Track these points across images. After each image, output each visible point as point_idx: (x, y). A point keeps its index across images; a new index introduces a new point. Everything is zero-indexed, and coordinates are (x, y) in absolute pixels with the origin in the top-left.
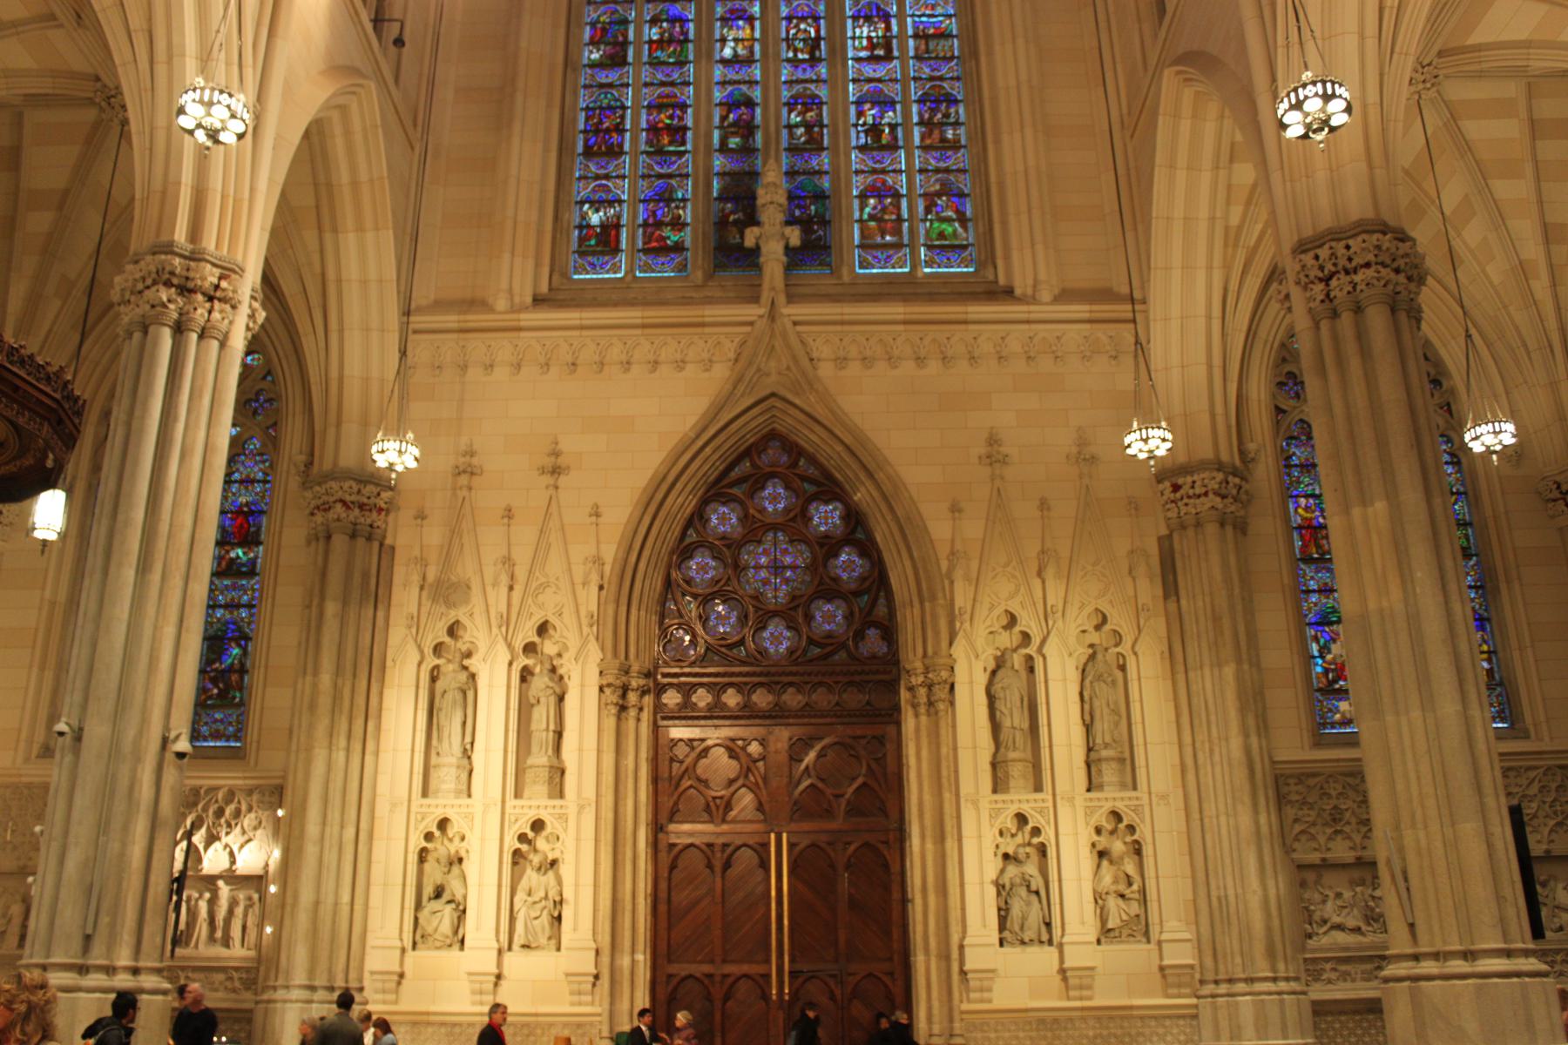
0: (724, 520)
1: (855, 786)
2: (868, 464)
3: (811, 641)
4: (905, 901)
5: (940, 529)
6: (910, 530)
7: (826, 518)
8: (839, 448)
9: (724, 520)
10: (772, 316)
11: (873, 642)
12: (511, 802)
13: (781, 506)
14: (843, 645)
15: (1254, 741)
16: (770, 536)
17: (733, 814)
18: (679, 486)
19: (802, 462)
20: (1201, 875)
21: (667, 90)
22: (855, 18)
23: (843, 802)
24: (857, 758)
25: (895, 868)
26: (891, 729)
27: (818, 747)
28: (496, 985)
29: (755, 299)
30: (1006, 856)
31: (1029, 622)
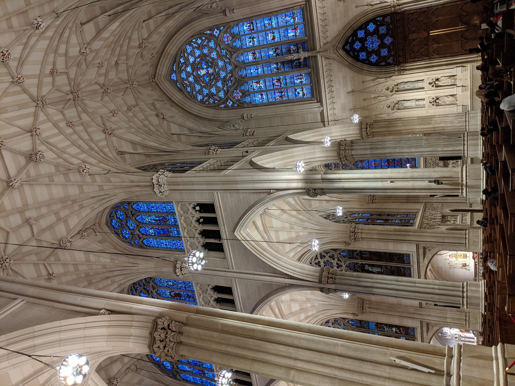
0: (363, 55)
7: (361, 34)
9: (363, 55)
10: (319, 52)
12: (425, 89)
28: (464, 86)
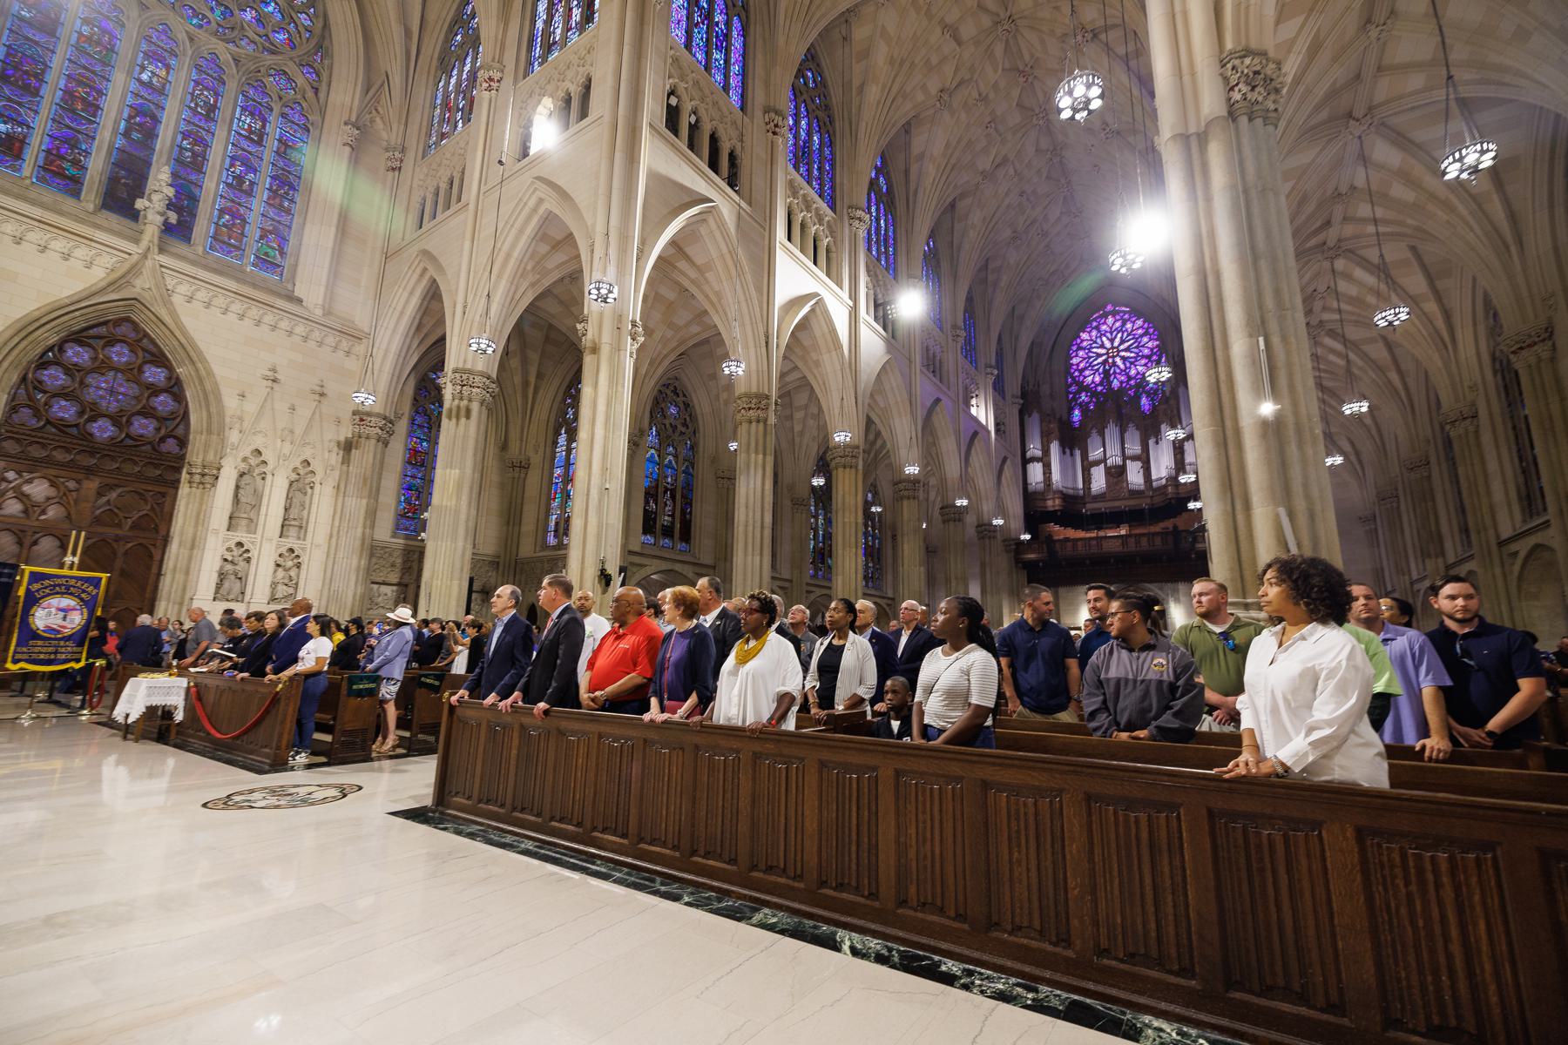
1: (141, 514)
2: (192, 355)
3: (128, 436)
4: (159, 574)
5: (230, 402)
6: (211, 397)
7: (154, 375)
8: (176, 343)
11: (170, 446)
13: (124, 359)
14: (150, 443)
15: (368, 530)
16: (112, 373)
17: (43, 517)
18: (48, 327)
19: (145, 341)
20: (327, 581)
21: (88, 74)
22: (244, 109)
23: (130, 521)
24: (146, 501)
25: (157, 558)
26: (171, 491)
27: (119, 490)
29: (137, 241)
30: (226, 560)
31: (268, 455)
